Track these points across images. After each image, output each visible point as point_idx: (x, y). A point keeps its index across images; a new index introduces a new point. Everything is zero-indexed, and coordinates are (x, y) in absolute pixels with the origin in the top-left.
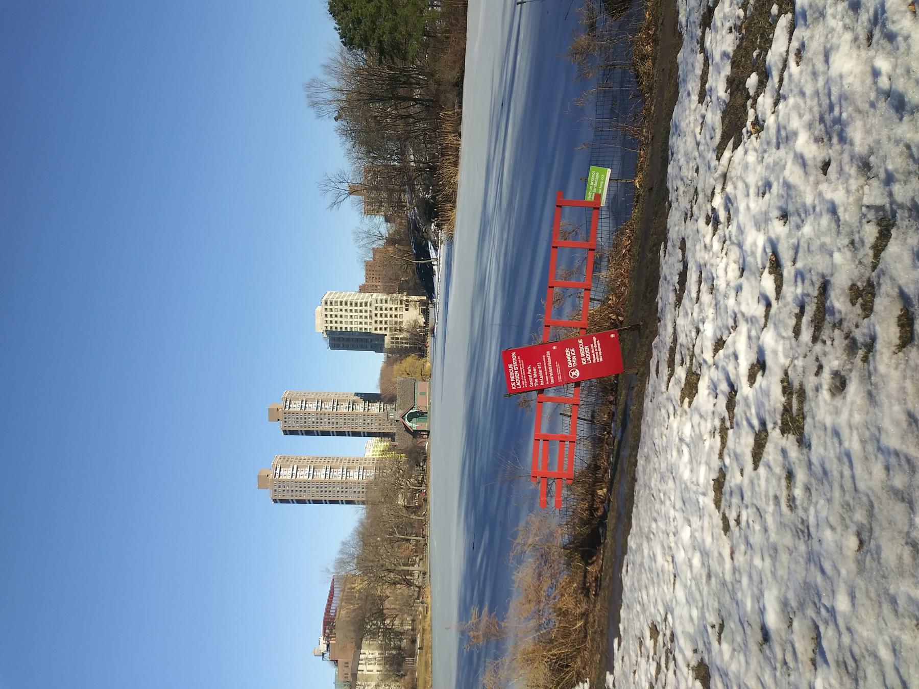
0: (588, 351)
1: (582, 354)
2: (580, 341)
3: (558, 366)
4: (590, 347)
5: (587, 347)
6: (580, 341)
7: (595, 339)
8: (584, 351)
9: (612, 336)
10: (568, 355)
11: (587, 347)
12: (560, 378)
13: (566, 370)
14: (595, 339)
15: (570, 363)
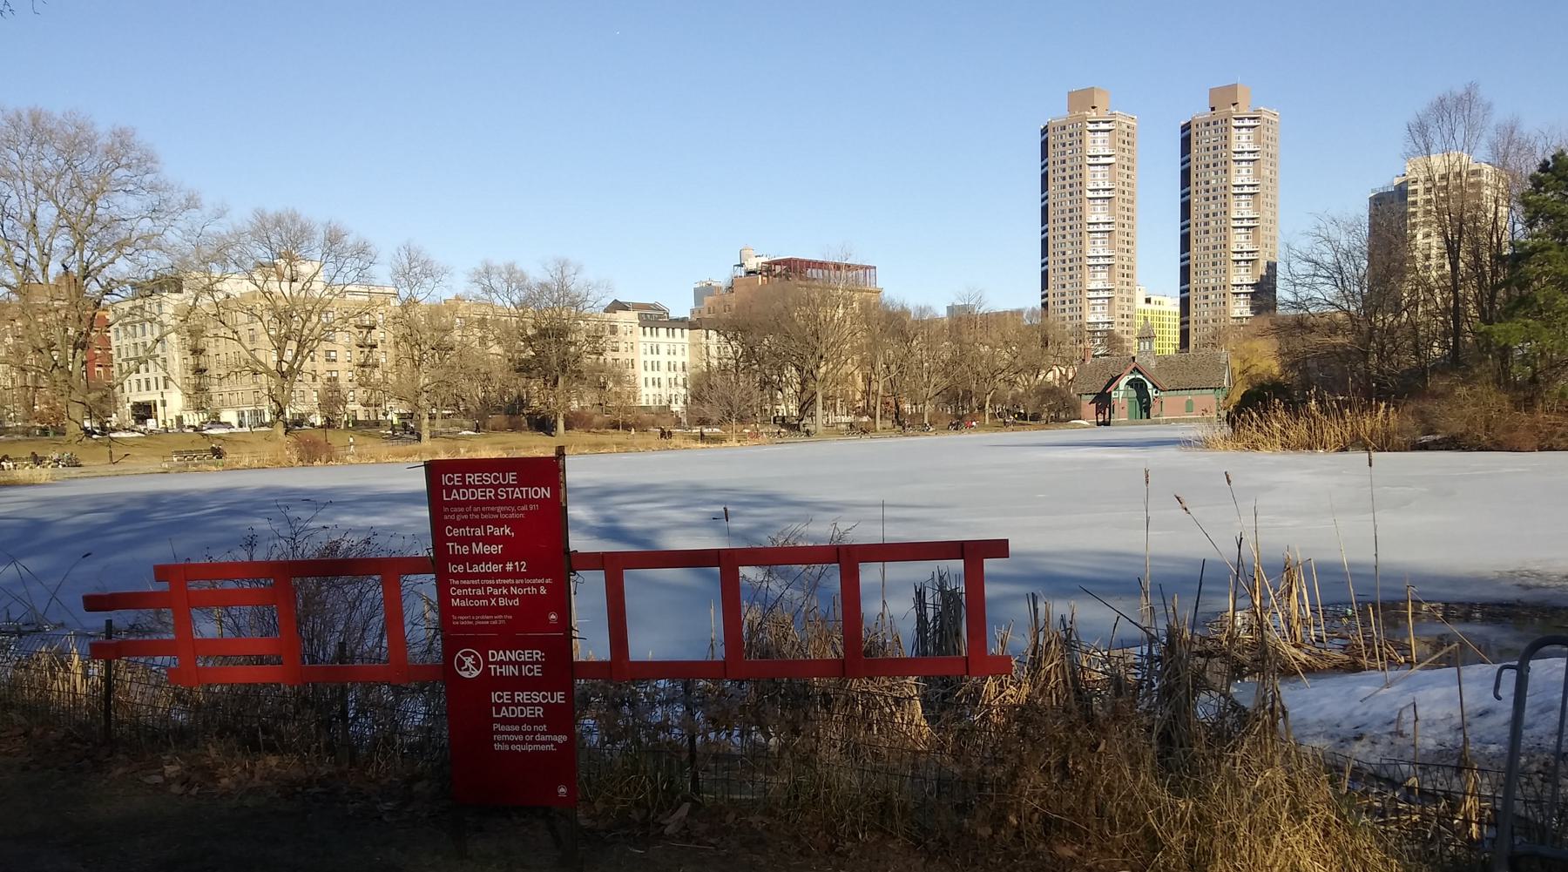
0: (528, 712)
1: (521, 696)
2: (559, 697)
3: (500, 619)
4: (538, 721)
5: (539, 712)
6: (559, 697)
7: (561, 739)
8: (531, 703)
9: (562, 790)
10: (526, 656)
11: (539, 712)
12: (464, 620)
13: (483, 642)
14: (561, 739)
15: (500, 656)
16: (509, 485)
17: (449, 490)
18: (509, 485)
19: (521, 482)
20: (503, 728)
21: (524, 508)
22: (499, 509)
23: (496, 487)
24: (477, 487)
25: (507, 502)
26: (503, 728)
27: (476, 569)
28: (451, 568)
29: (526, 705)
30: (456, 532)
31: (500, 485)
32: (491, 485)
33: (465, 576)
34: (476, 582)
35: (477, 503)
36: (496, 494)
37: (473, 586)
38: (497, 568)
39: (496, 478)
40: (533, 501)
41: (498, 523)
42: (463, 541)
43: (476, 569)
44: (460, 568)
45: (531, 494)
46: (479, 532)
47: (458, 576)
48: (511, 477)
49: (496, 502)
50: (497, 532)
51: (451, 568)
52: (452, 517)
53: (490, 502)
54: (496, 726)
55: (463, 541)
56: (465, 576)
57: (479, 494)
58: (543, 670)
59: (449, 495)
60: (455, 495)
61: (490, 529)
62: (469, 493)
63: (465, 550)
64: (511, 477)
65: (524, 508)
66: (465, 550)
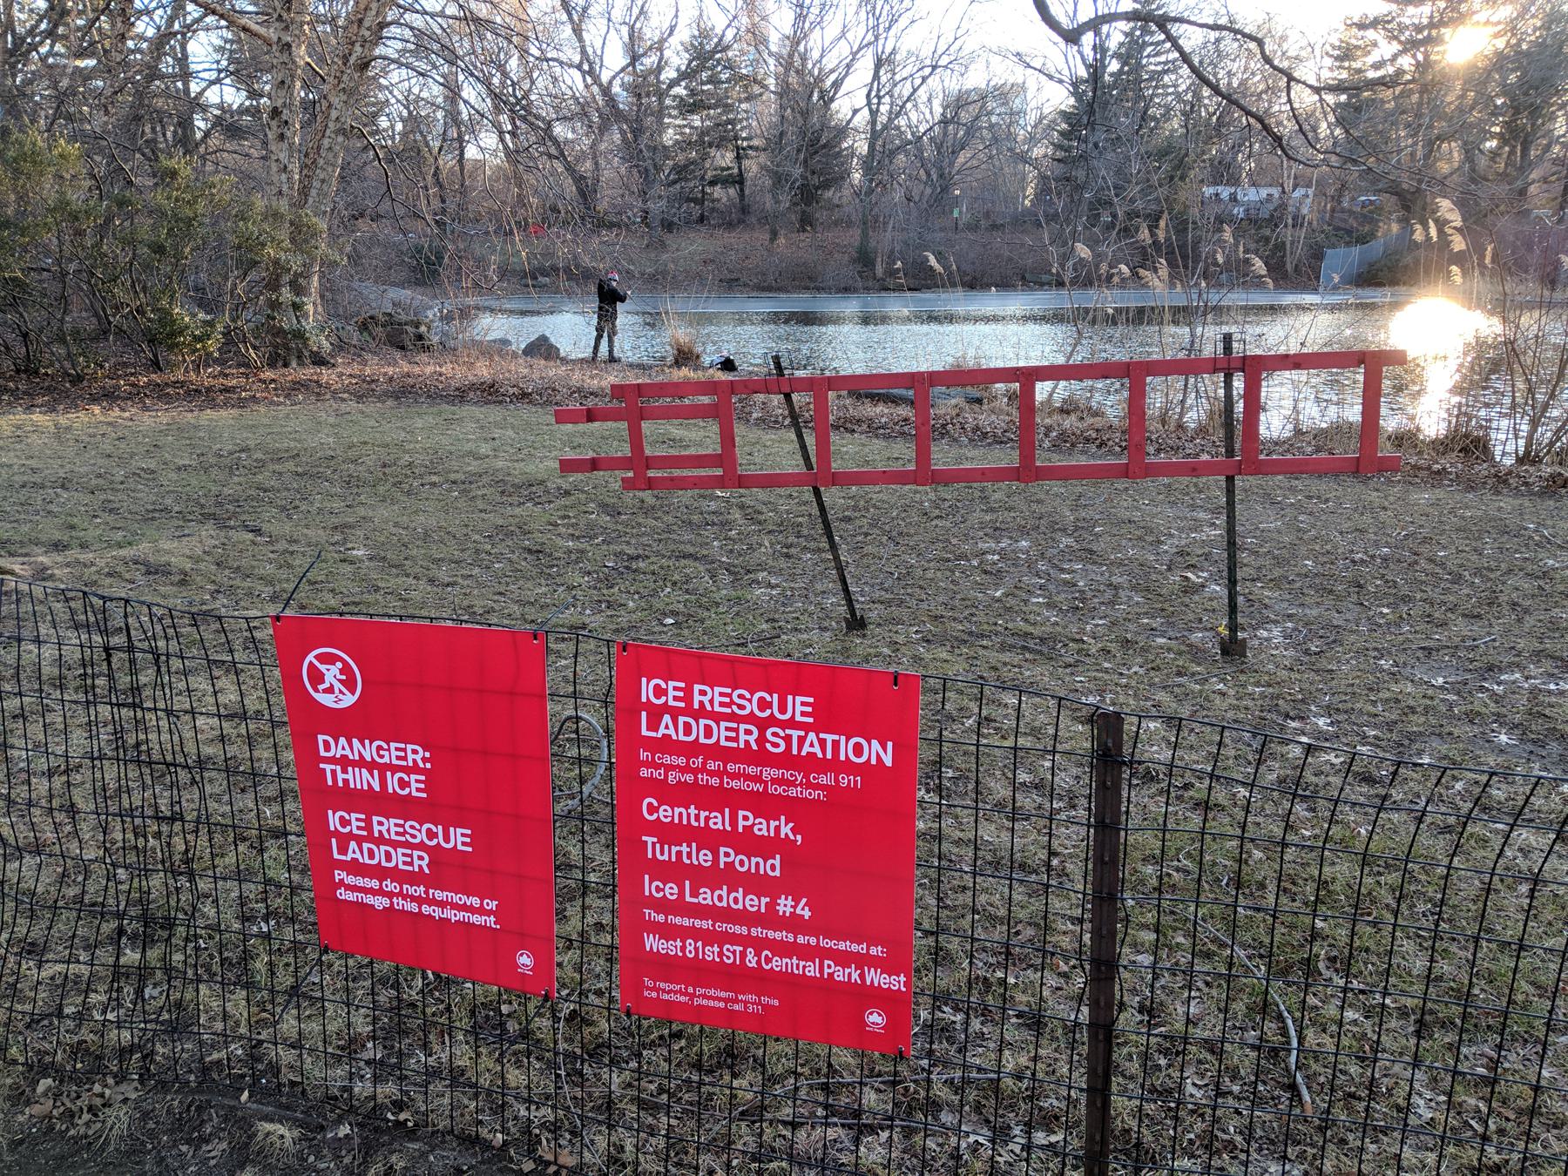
17: (656, 715)
18: (792, 723)
21: (824, 780)
22: (769, 773)
23: (763, 725)
24: (718, 717)
25: (786, 760)
27: (706, 897)
28: (650, 887)
32: (751, 719)
33: (679, 907)
34: (706, 924)
35: (716, 752)
36: (762, 740)
37: (695, 934)
38: (753, 903)
39: (763, 705)
40: (849, 767)
43: (706, 897)
44: (671, 891)
45: (846, 750)
46: (718, 822)
48: (799, 706)
49: (761, 756)
50: (762, 828)
52: (658, 774)
53: (745, 755)
56: (679, 907)
59: (653, 726)
60: (666, 727)
61: (745, 819)
64: (799, 706)
65: (824, 780)
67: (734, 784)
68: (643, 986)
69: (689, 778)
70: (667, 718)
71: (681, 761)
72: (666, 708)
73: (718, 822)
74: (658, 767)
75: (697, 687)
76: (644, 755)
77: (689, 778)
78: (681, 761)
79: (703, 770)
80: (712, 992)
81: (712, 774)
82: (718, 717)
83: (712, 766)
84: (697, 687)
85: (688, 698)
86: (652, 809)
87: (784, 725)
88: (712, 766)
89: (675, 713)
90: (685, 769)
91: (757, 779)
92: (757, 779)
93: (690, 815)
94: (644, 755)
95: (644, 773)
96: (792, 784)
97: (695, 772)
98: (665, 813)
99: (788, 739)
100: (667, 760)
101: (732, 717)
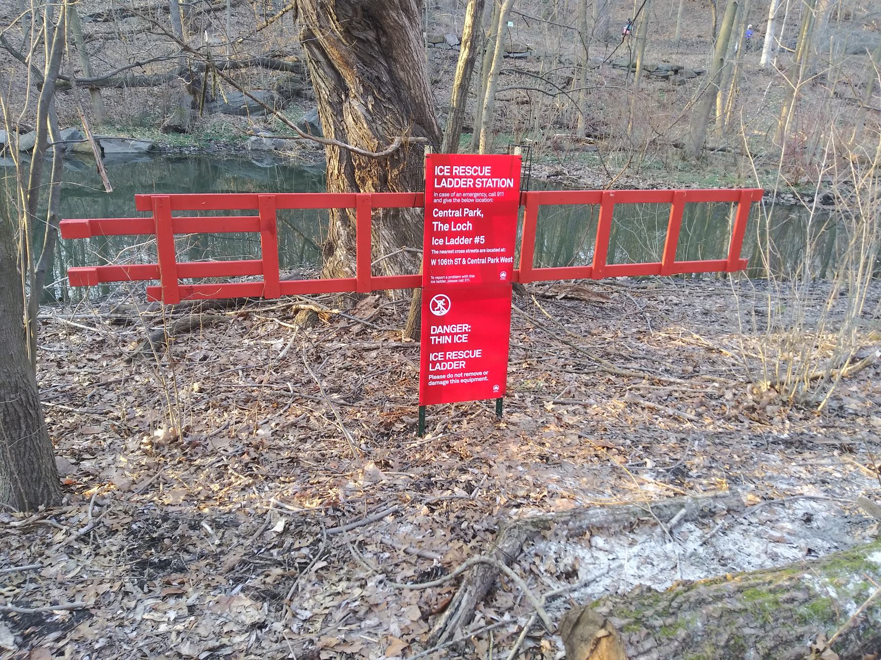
16: (484, 177)
18: (484, 177)
19: (494, 174)
20: (435, 377)
22: (476, 195)
23: (475, 178)
24: (460, 177)
25: (482, 190)
26: (435, 377)
27: (453, 242)
29: (453, 361)
30: (441, 214)
31: (478, 176)
33: (444, 247)
35: (460, 190)
36: (474, 184)
39: (476, 171)
41: (473, 206)
42: (444, 220)
43: (453, 242)
44: (441, 242)
46: (458, 214)
47: (439, 248)
48: (486, 170)
49: (474, 190)
51: (434, 242)
52: (440, 201)
54: (430, 377)
55: (444, 220)
56: (444, 247)
57: (462, 183)
58: (469, 338)
59: (439, 184)
60: (444, 184)
62: (454, 182)
63: (446, 227)
64: (486, 170)
66: (446, 227)
67: (465, 201)
68: (431, 279)
69: (450, 200)
70: (444, 180)
71: (448, 195)
72: (444, 176)
73: (458, 214)
74: (439, 198)
75: (454, 167)
76: (435, 194)
77: (450, 200)
78: (448, 195)
79: (455, 197)
80: (454, 277)
81: (458, 198)
82: (460, 177)
83: (458, 195)
84: (454, 167)
85: (451, 172)
86: (436, 213)
87: (481, 177)
88: (458, 195)
89: (446, 178)
90: (448, 198)
91: (472, 198)
92: (472, 198)
93: (449, 213)
94: (435, 194)
95: (435, 201)
96: (483, 198)
97: (452, 198)
98: (441, 214)
99: (482, 182)
100: (443, 195)
101: (466, 177)
